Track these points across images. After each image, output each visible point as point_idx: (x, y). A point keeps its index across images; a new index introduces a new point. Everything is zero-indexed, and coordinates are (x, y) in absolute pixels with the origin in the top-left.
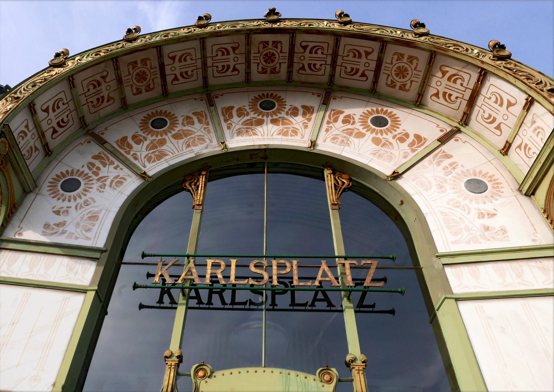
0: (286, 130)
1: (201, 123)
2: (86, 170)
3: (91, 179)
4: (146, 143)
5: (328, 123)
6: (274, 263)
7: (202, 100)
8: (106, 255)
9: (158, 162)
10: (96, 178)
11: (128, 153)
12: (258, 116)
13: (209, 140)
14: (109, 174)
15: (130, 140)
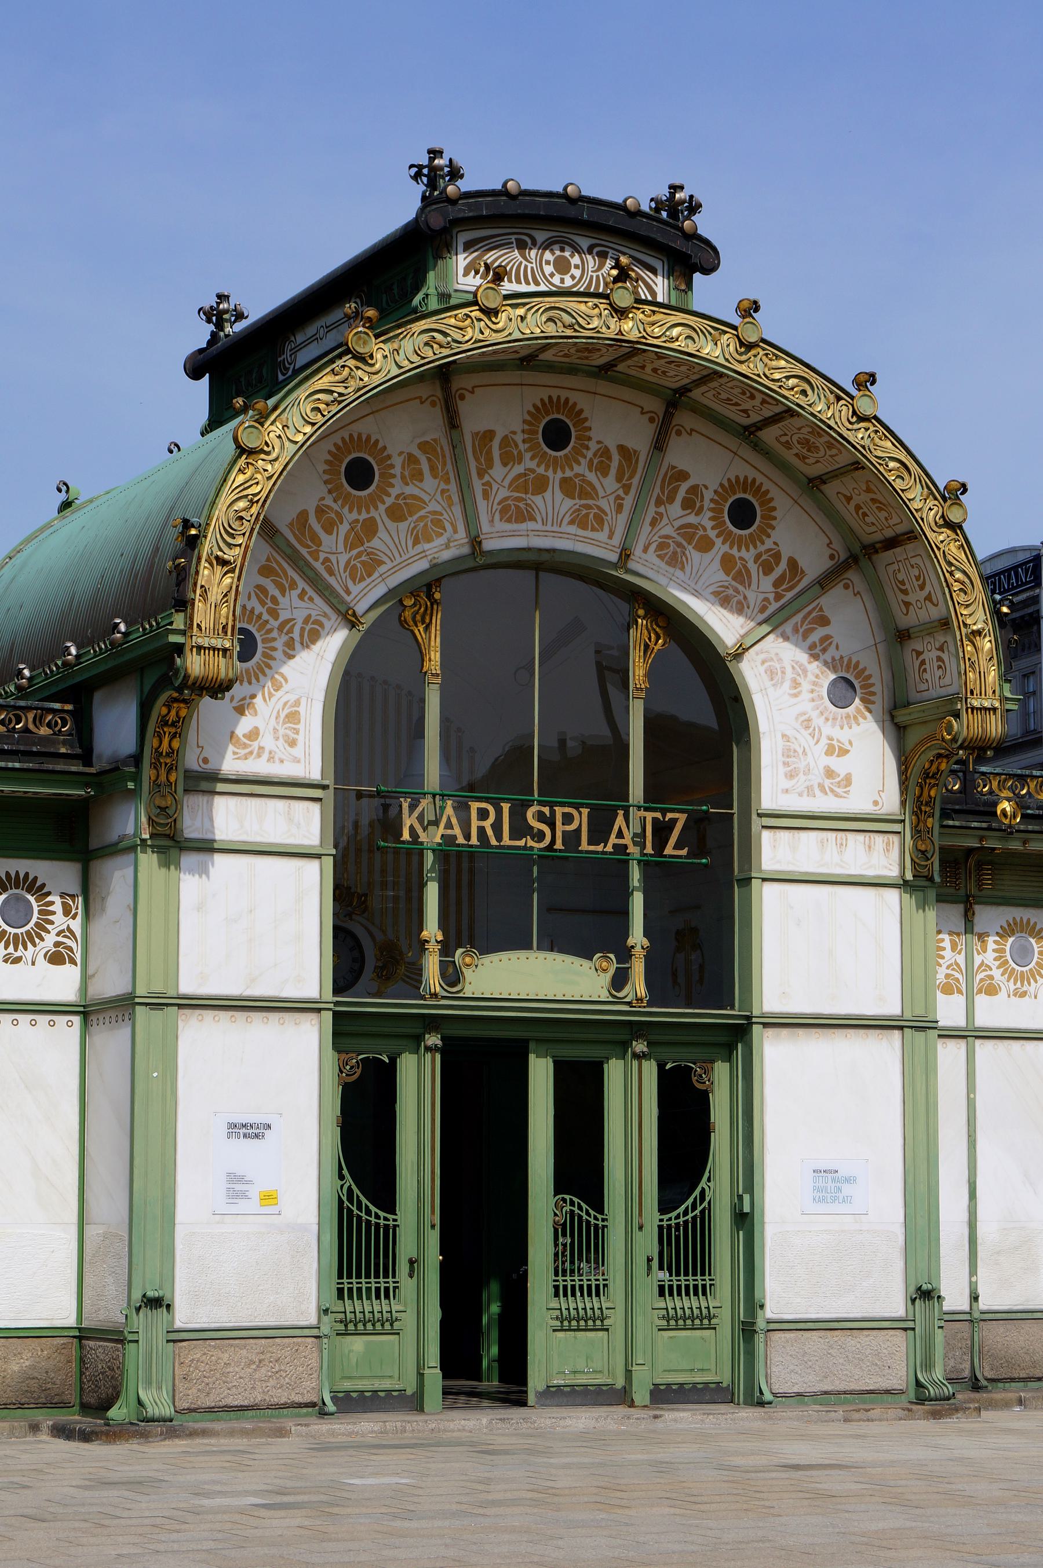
0: (584, 512)
1: (435, 477)
3: (268, 626)
4: (344, 528)
5: (659, 502)
6: (559, 811)
9: (368, 580)
10: (274, 624)
11: (317, 559)
12: (538, 466)
13: (452, 524)
15: (312, 520)
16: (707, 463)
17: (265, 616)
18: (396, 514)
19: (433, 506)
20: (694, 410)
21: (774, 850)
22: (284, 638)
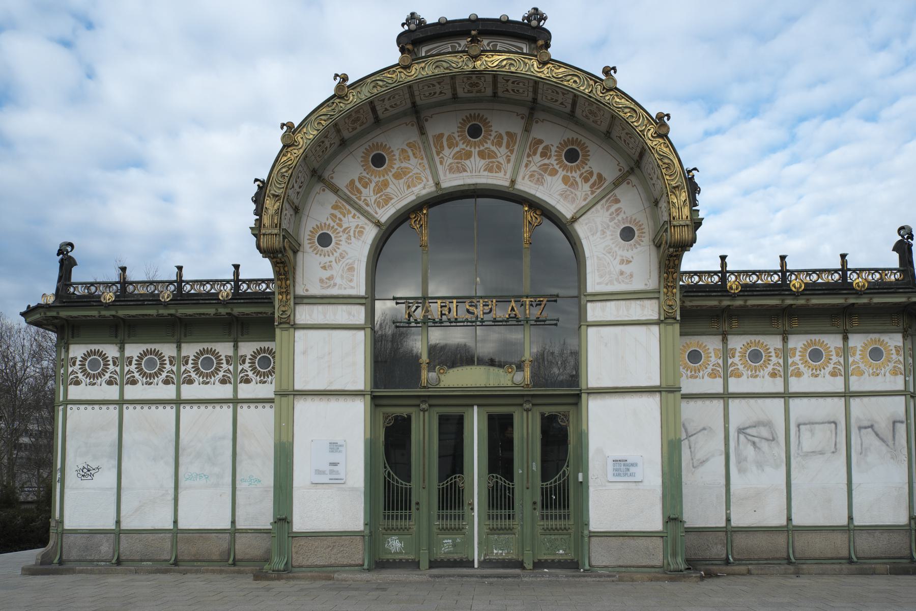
2: (330, 222)
4: (373, 185)
7: (413, 125)
8: (369, 300)
14: (351, 224)
15: (357, 183)
16: (552, 135)
17: (336, 227)
18: (397, 176)
19: (416, 171)
20: (543, 111)
21: (594, 312)
22: (346, 236)
